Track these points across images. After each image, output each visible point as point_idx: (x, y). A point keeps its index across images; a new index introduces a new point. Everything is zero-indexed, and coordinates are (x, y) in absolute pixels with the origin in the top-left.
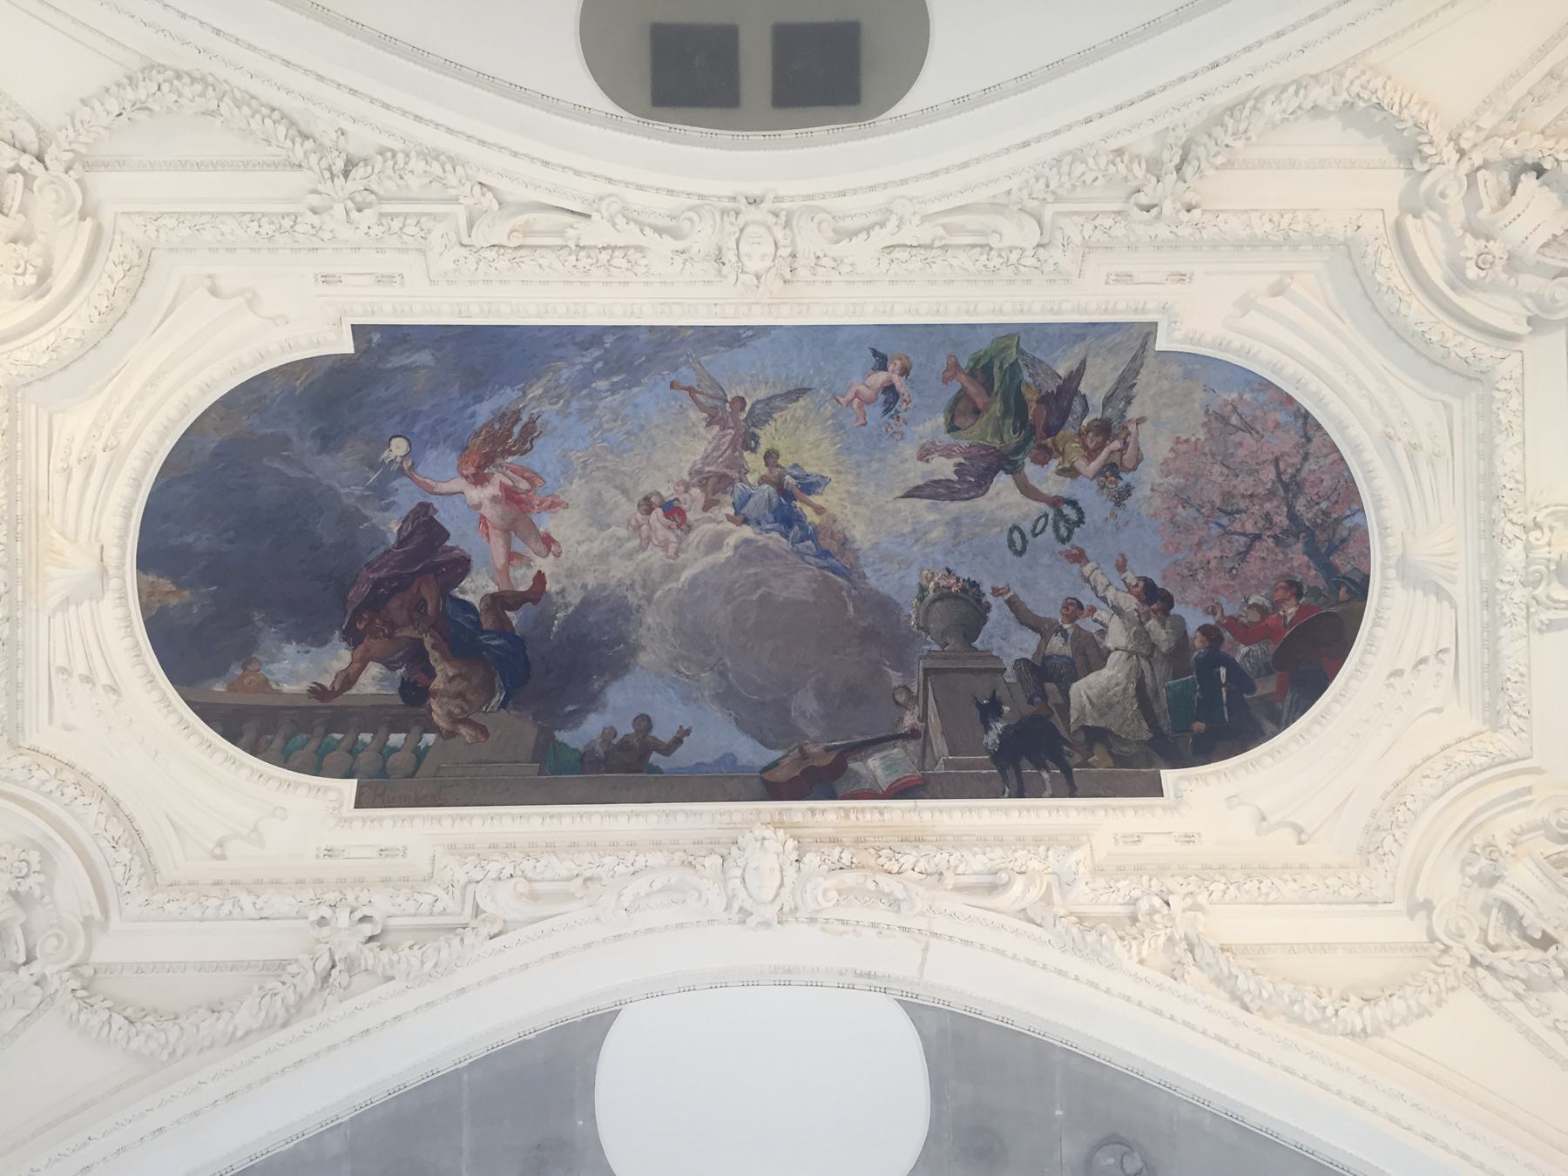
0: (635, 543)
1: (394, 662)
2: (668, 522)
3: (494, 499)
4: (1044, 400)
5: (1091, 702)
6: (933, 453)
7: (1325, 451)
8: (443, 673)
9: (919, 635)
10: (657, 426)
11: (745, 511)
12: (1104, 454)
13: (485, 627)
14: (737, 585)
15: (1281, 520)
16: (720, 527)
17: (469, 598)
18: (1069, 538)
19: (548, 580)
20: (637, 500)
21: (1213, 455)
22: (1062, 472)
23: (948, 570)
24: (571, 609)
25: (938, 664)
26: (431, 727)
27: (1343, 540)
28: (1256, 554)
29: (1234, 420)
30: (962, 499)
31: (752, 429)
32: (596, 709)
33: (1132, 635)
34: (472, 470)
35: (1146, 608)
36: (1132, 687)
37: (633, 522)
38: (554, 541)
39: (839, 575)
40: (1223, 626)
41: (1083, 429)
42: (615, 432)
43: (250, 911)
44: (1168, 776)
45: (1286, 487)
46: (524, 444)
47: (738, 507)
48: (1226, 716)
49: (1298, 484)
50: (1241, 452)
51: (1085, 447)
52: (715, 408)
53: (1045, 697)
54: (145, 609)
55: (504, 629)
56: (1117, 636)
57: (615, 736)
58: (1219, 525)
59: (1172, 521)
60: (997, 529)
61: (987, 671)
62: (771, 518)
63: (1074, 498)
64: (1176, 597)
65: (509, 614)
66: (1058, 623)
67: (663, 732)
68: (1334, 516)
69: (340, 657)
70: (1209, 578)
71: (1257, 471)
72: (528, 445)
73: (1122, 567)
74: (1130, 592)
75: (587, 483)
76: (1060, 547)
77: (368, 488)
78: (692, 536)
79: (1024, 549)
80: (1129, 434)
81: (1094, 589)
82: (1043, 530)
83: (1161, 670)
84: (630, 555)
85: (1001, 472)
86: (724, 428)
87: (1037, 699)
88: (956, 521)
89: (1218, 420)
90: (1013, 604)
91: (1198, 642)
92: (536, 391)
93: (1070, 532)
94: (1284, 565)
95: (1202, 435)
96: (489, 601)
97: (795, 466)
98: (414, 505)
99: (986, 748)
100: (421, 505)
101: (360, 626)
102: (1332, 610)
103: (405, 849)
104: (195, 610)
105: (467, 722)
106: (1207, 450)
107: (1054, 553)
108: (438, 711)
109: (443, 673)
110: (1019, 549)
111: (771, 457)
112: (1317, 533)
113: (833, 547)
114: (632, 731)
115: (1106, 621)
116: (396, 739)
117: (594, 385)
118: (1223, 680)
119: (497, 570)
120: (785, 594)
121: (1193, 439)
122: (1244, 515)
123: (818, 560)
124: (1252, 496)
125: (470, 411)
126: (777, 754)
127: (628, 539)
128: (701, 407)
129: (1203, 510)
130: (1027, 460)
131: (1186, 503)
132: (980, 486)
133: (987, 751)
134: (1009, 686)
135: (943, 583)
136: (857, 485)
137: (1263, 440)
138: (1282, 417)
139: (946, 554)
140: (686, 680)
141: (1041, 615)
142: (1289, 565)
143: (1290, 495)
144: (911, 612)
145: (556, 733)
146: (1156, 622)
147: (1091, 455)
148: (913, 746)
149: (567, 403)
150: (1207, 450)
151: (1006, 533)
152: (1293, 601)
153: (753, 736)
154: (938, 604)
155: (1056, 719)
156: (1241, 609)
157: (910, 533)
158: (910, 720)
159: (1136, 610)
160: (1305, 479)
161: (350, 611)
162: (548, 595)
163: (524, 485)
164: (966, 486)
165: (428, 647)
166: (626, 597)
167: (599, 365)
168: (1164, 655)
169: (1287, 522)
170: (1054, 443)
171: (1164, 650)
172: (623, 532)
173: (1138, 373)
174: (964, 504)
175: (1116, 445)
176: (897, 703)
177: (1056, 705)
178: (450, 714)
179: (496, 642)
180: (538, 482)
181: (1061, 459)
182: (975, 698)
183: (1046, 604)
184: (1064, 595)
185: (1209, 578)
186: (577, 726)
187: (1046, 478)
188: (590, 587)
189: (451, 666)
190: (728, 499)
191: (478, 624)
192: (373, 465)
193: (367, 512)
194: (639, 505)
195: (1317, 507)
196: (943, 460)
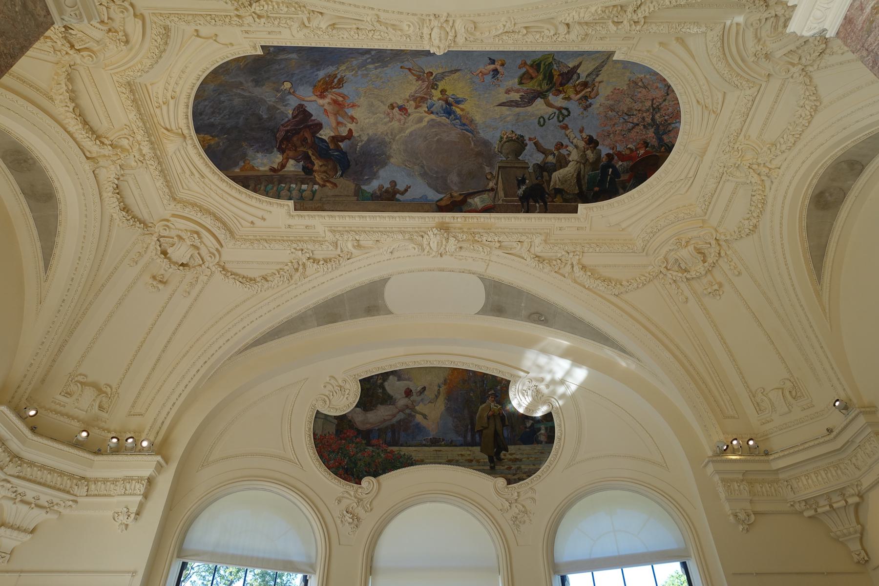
0: (389, 119)
1: (299, 159)
3: (329, 103)
4: (561, 75)
5: (559, 180)
7: (673, 99)
8: (317, 164)
9: (498, 154)
10: (395, 80)
11: (432, 109)
12: (583, 92)
13: (331, 148)
14: (428, 135)
15: (648, 120)
16: (421, 115)
17: (323, 137)
18: (563, 121)
19: (353, 131)
20: (388, 105)
21: (628, 95)
22: (565, 98)
23: (513, 132)
24: (363, 142)
26: (315, 183)
27: (669, 131)
28: (635, 131)
29: (640, 84)
30: (521, 107)
31: (435, 82)
32: (376, 179)
34: (319, 93)
36: (575, 175)
37: (386, 112)
39: (469, 132)
42: (377, 82)
43: (268, 248)
44: (581, 207)
45: (654, 109)
46: (340, 85)
47: (429, 108)
48: (607, 186)
49: (658, 109)
50: (639, 95)
51: (576, 91)
53: (542, 177)
54: (203, 147)
55: (338, 149)
56: (574, 156)
58: (624, 119)
59: (605, 116)
61: (522, 167)
62: (442, 112)
68: (669, 122)
69: (278, 158)
70: (615, 136)
72: (341, 85)
73: (581, 131)
74: (583, 140)
75: (367, 98)
77: (277, 99)
78: (410, 117)
79: (544, 124)
80: (595, 86)
81: (569, 139)
84: (386, 124)
85: (539, 98)
86: (423, 82)
87: (539, 178)
88: (518, 114)
92: (343, 67)
93: (564, 119)
96: (331, 138)
97: (453, 95)
98: (296, 105)
99: (518, 195)
100: (299, 104)
101: (284, 146)
103: (314, 226)
104: (221, 144)
107: (556, 126)
109: (317, 164)
110: (542, 124)
111: (443, 92)
113: (467, 122)
114: (389, 186)
116: (304, 187)
117: (367, 66)
119: (333, 128)
120: (447, 138)
121: (621, 89)
122: (634, 117)
124: (639, 110)
125: (316, 73)
126: (442, 196)
127: (385, 118)
128: (414, 75)
129: (619, 113)
130: (551, 94)
131: (612, 110)
133: (518, 196)
135: (509, 136)
136: (478, 101)
137: (650, 92)
138: (659, 85)
140: (408, 168)
141: (546, 148)
143: (654, 112)
144: (496, 146)
145: (362, 186)
147: (577, 93)
148: (492, 194)
149: (357, 72)
151: (538, 119)
152: (644, 149)
153: (434, 189)
154: (507, 143)
155: (545, 185)
157: (499, 118)
158: (491, 184)
159: (584, 147)
160: (662, 108)
161: (279, 141)
162: (354, 137)
163: (340, 99)
164: (523, 102)
165: (310, 154)
166: (384, 138)
167: (370, 60)
169: (650, 121)
170: (563, 89)
171: (591, 161)
172: (382, 116)
175: (589, 90)
176: (487, 178)
177: (546, 180)
178: (322, 178)
179: (336, 153)
180: (346, 98)
183: (550, 145)
184: (557, 141)
185: (615, 136)
186: (370, 183)
187: (558, 101)
188: (370, 135)
189: (320, 161)
191: (328, 147)
192: (278, 91)
193: (279, 107)
194: (388, 107)
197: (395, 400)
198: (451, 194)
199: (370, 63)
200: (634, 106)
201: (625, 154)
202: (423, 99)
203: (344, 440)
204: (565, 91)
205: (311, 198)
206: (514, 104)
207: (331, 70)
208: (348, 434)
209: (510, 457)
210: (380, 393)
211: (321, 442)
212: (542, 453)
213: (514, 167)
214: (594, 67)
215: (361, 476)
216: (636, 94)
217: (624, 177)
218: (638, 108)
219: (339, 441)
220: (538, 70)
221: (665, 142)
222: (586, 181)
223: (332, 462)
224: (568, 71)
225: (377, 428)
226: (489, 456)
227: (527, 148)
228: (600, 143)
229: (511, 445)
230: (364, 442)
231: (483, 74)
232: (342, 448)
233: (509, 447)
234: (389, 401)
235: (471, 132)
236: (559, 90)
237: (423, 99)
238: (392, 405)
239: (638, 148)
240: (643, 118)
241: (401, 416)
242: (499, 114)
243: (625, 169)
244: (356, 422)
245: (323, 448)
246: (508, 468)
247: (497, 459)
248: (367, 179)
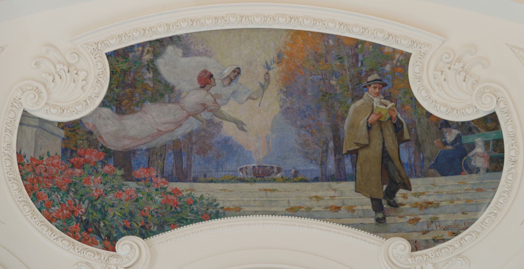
197: (180, 94)
203: (78, 168)
208: (87, 156)
209: (415, 200)
210: (149, 79)
211: (34, 171)
212: (479, 190)
215: (115, 235)
219: (70, 171)
223: (57, 208)
225: (144, 147)
226: (372, 199)
229: (417, 177)
230: (119, 172)
232: (75, 184)
233: (413, 181)
234: (166, 96)
238: (173, 103)
244: (103, 136)
245: (38, 181)
246: (412, 220)
247: (389, 204)
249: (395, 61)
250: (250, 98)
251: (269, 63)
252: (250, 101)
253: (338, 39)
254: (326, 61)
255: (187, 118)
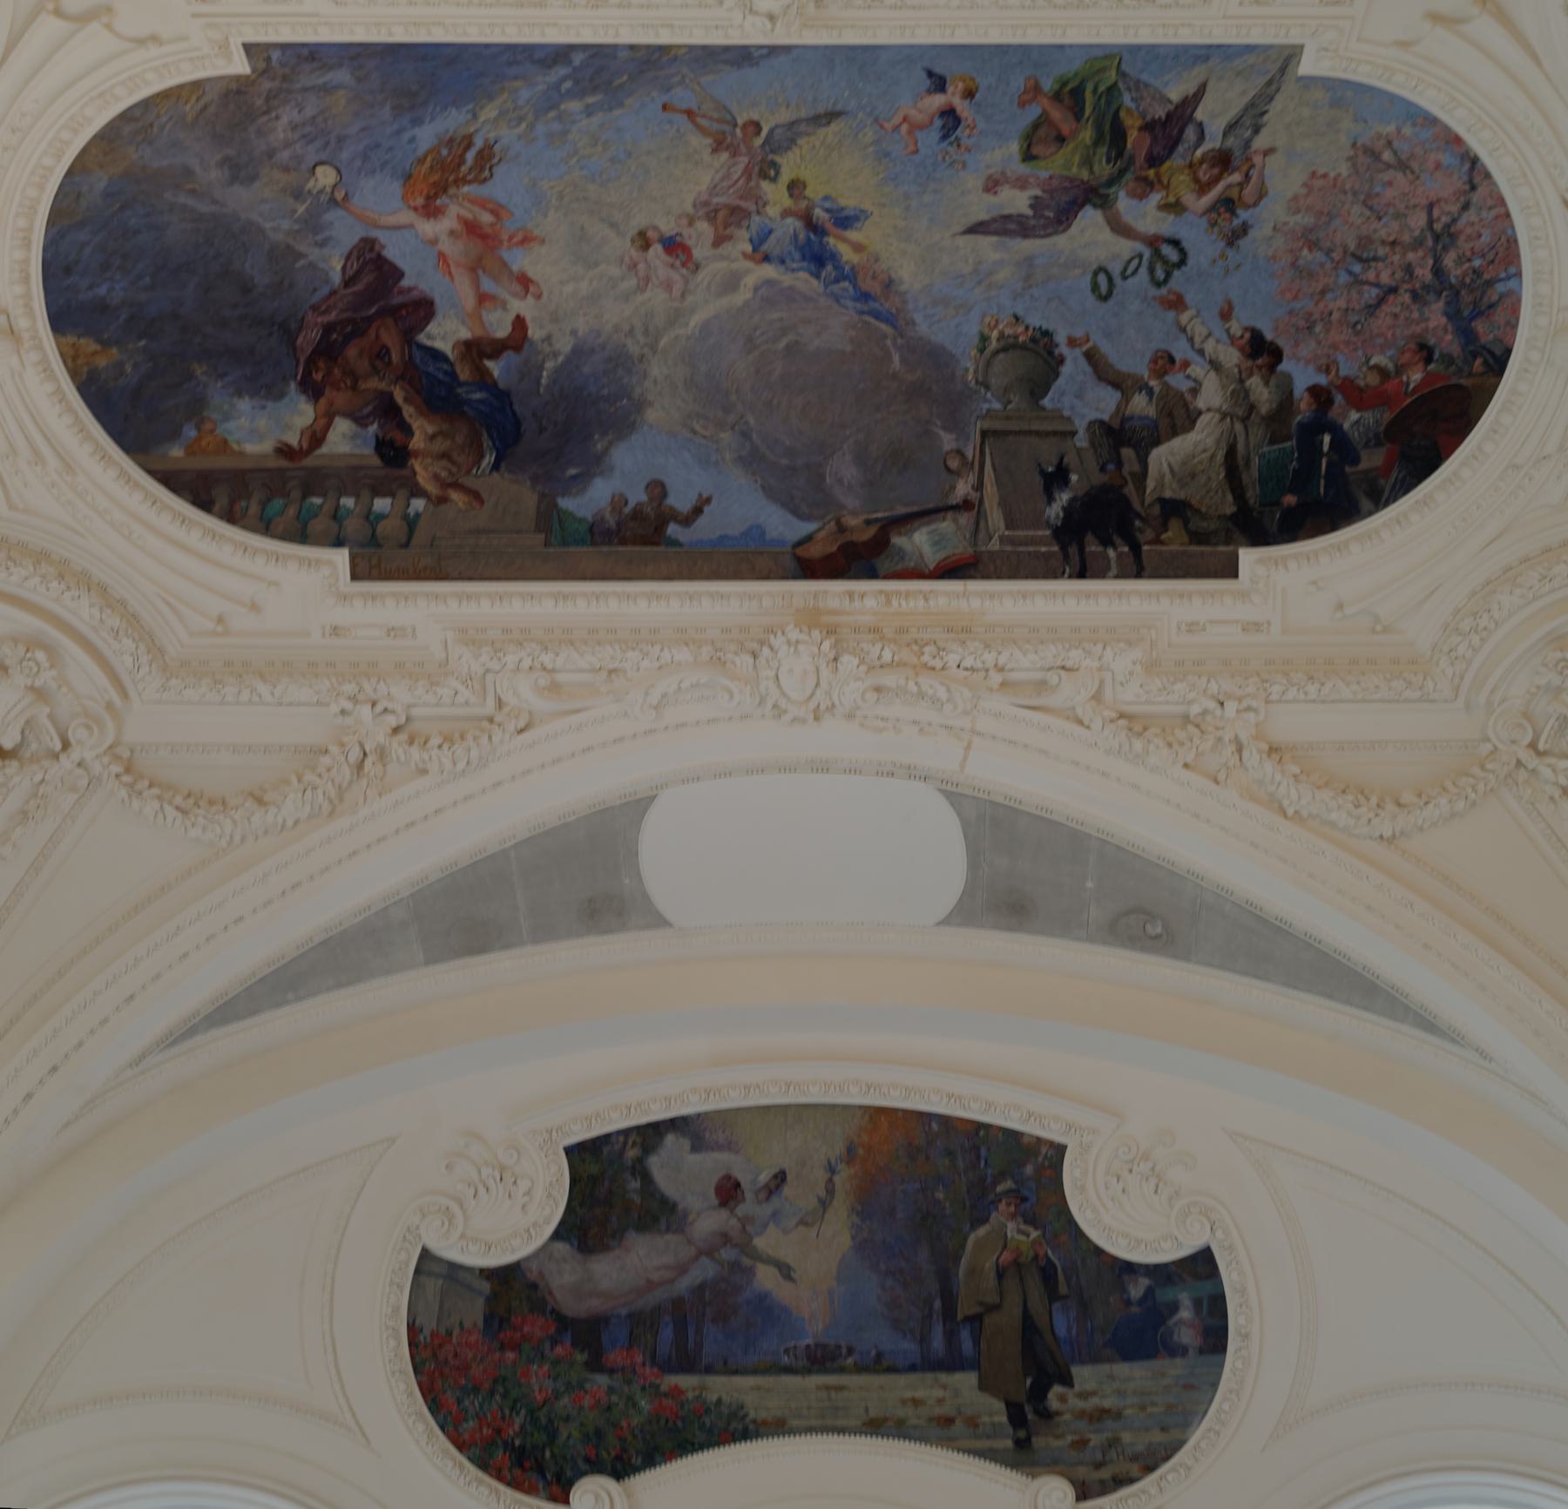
0: (633, 282)
2: (670, 259)
4: (1149, 127)
6: (1002, 184)
7: (1490, 202)
8: (422, 431)
11: (765, 247)
14: (758, 333)
15: (1424, 273)
18: (1166, 281)
21: (1355, 194)
22: (1165, 207)
23: (1017, 318)
24: (561, 359)
25: (998, 425)
26: (417, 491)
27: (1491, 306)
29: (1387, 156)
31: (770, 157)
33: (1228, 394)
35: (1250, 363)
37: (627, 259)
38: (532, 281)
40: (1338, 387)
41: (1195, 160)
44: (1248, 557)
45: (1437, 238)
47: (757, 243)
49: (1451, 236)
50: (1390, 193)
51: (1196, 180)
52: (724, 133)
53: (1119, 464)
56: (1212, 395)
57: (626, 503)
58: (1350, 273)
59: (1293, 265)
60: (1077, 271)
61: (1055, 433)
62: (797, 256)
63: (1177, 237)
64: (1287, 352)
65: (489, 364)
66: (1142, 377)
67: (680, 501)
68: (1486, 276)
70: (1328, 331)
71: (1405, 216)
73: (1226, 315)
74: (1232, 343)
76: (1153, 292)
80: (1253, 166)
81: (1191, 340)
82: (1136, 270)
83: (1258, 433)
86: (734, 154)
87: (1111, 467)
88: (1029, 261)
89: (1368, 155)
90: (1092, 357)
91: (1304, 407)
93: (1168, 275)
94: (1417, 324)
95: (1344, 169)
97: (826, 198)
102: (1463, 382)
105: (456, 485)
106: (1348, 187)
108: (423, 472)
109: (422, 431)
111: (795, 187)
112: (1463, 292)
113: (874, 288)
114: (644, 498)
115: (1200, 377)
118: (1326, 448)
121: (1332, 174)
122: (1380, 265)
123: (859, 305)
124: (1393, 243)
126: (810, 527)
127: (623, 279)
128: (704, 131)
129: (1334, 255)
130: (1122, 194)
131: (1313, 245)
132: (1060, 222)
134: (1079, 451)
135: (1008, 331)
137: (1418, 182)
138: (1446, 159)
139: (1015, 299)
142: (1423, 325)
143: (1440, 247)
144: (968, 365)
146: (1259, 380)
147: (1203, 188)
148: (965, 519)
150: (1348, 187)
151: (1089, 277)
152: (1421, 365)
153: (784, 505)
154: (1002, 356)
155: (1130, 490)
156: (1360, 368)
158: (963, 488)
160: (1460, 232)
164: (1042, 222)
166: (624, 346)
168: (1263, 418)
170: (1158, 175)
171: (1264, 409)
172: (615, 271)
173: (1272, 99)
174: (1038, 242)
175: (1236, 178)
177: (1132, 474)
181: (1164, 193)
182: (1040, 465)
183: (1132, 359)
187: (1146, 215)
188: (580, 334)
190: (745, 234)
194: (633, 241)
195: (1467, 265)
196: (1017, 193)
198: (838, 523)
199: (570, 95)
200: (1375, 231)
201: (1367, 386)
202: (736, 215)
204: (1165, 182)
205: (404, 540)
206: (1012, 226)
207: (452, 121)
213: (1030, 433)
214: (1246, 100)
216: (1378, 189)
217: (1372, 459)
218: (1389, 235)
220: (1077, 112)
221: (1483, 340)
222: (1256, 474)
224: (1169, 115)
225: (624, 1312)
227: (1066, 369)
228: (1285, 354)
230: (581, 1357)
231: (915, 127)
235: (890, 319)
236: (1145, 180)
237: (736, 215)
239: (1402, 366)
240: (1409, 269)
241: (705, 1271)
242: (971, 261)
243: (1371, 435)
248: (574, 477)
249: (1040, 1159)
250: (802, 1222)
251: (833, 1162)
252: (801, 1228)
253: (946, 1121)
254: (927, 1158)
255: (697, 1257)
